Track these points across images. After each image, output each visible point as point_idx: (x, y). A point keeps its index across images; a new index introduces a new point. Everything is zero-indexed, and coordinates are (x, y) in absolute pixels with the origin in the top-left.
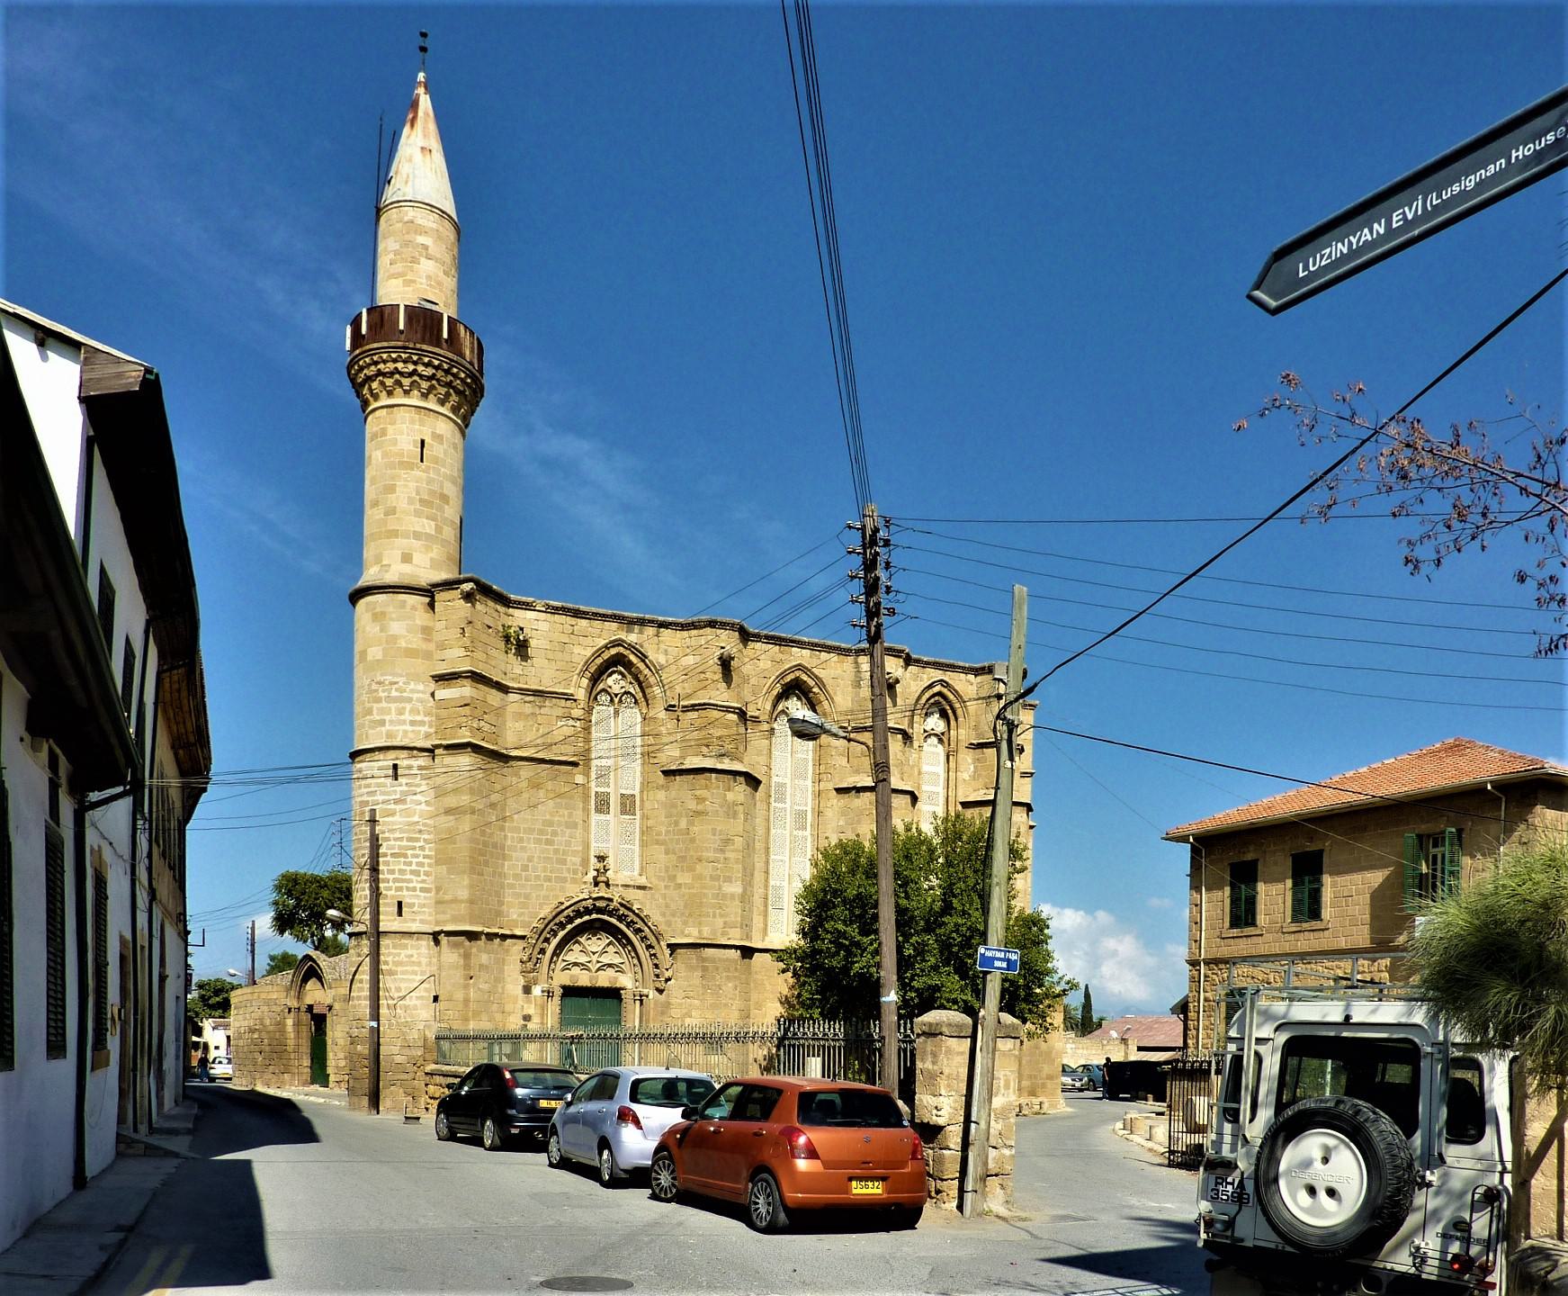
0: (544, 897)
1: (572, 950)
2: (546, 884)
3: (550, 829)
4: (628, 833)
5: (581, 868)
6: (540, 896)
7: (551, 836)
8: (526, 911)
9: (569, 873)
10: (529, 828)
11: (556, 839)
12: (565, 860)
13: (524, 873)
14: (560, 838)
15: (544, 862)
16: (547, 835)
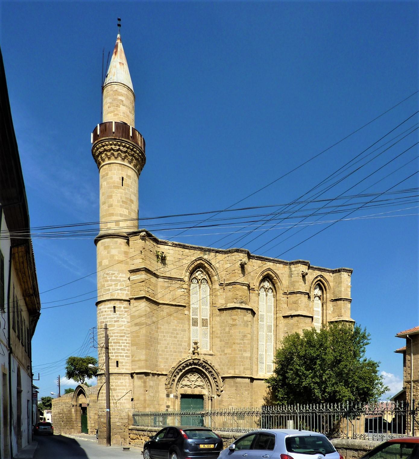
0: (174, 359)
3: (175, 332)
5: (188, 347)
9: (183, 349)
11: (178, 336)
15: (173, 345)
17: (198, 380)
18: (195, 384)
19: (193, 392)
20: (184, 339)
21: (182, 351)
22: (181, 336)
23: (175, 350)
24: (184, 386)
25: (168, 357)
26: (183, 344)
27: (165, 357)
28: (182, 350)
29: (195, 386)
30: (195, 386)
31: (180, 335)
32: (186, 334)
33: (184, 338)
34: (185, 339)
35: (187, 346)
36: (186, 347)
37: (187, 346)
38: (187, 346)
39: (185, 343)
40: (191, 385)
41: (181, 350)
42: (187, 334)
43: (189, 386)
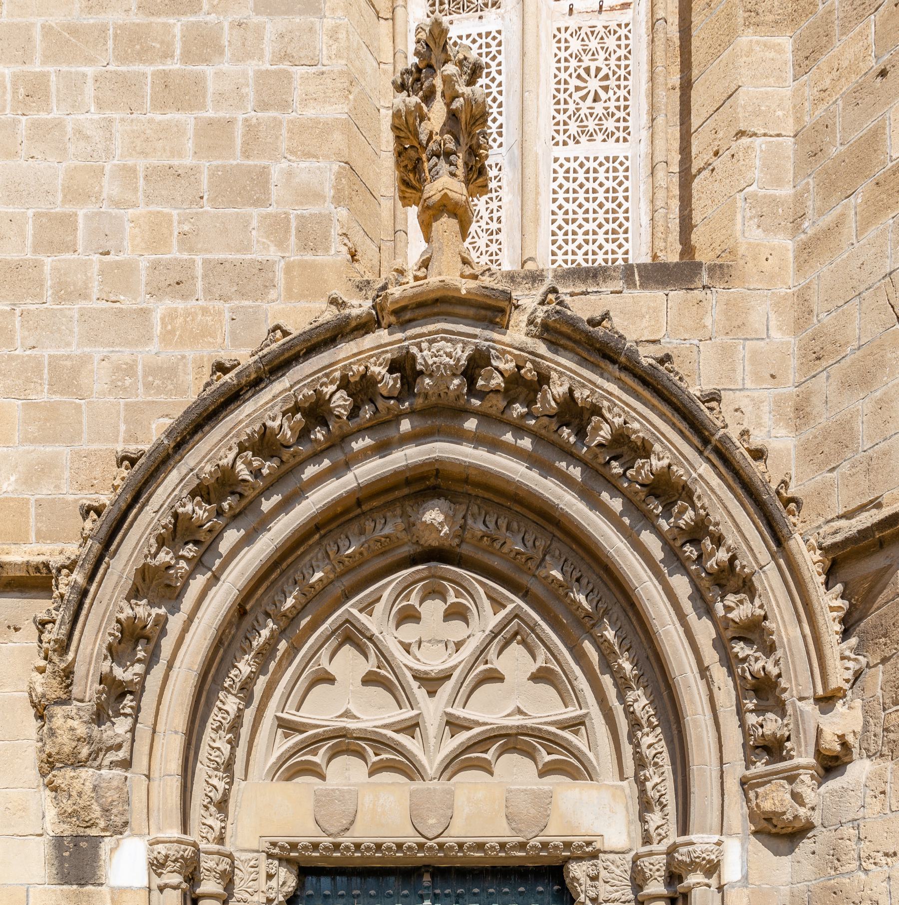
0: (152, 370)
1: (328, 679)
2: (161, 308)
3: (177, 25)
4: (594, 84)
5: (342, 213)
6: (130, 369)
7: (188, 56)
8: (63, 451)
9: (281, 244)
10: (74, 30)
11: (209, 71)
12: (264, 173)
13: (48, 262)
14: (226, 67)
16: (167, 55)
17: (501, 664)
18: (458, 711)
19: (432, 824)
20: (285, 105)
21: (263, 267)
22: (252, 67)
23: (175, 253)
24: (319, 759)
25: (85, 360)
26: (277, 170)
27: (46, 353)
28: (273, 253)
29: (463, 736)
30: (463, 736)
31: (244, 54)
32: (322, 42)
33: (297, 95)
34: (305, 102)
35: (338, 200)
36: (328, 207)
37: (330, 193)
38: (338, 200)
39: (308, 155)
40: (411, 727)
41: (247, 249)
42: (333, 34)
43: (379, 743)
